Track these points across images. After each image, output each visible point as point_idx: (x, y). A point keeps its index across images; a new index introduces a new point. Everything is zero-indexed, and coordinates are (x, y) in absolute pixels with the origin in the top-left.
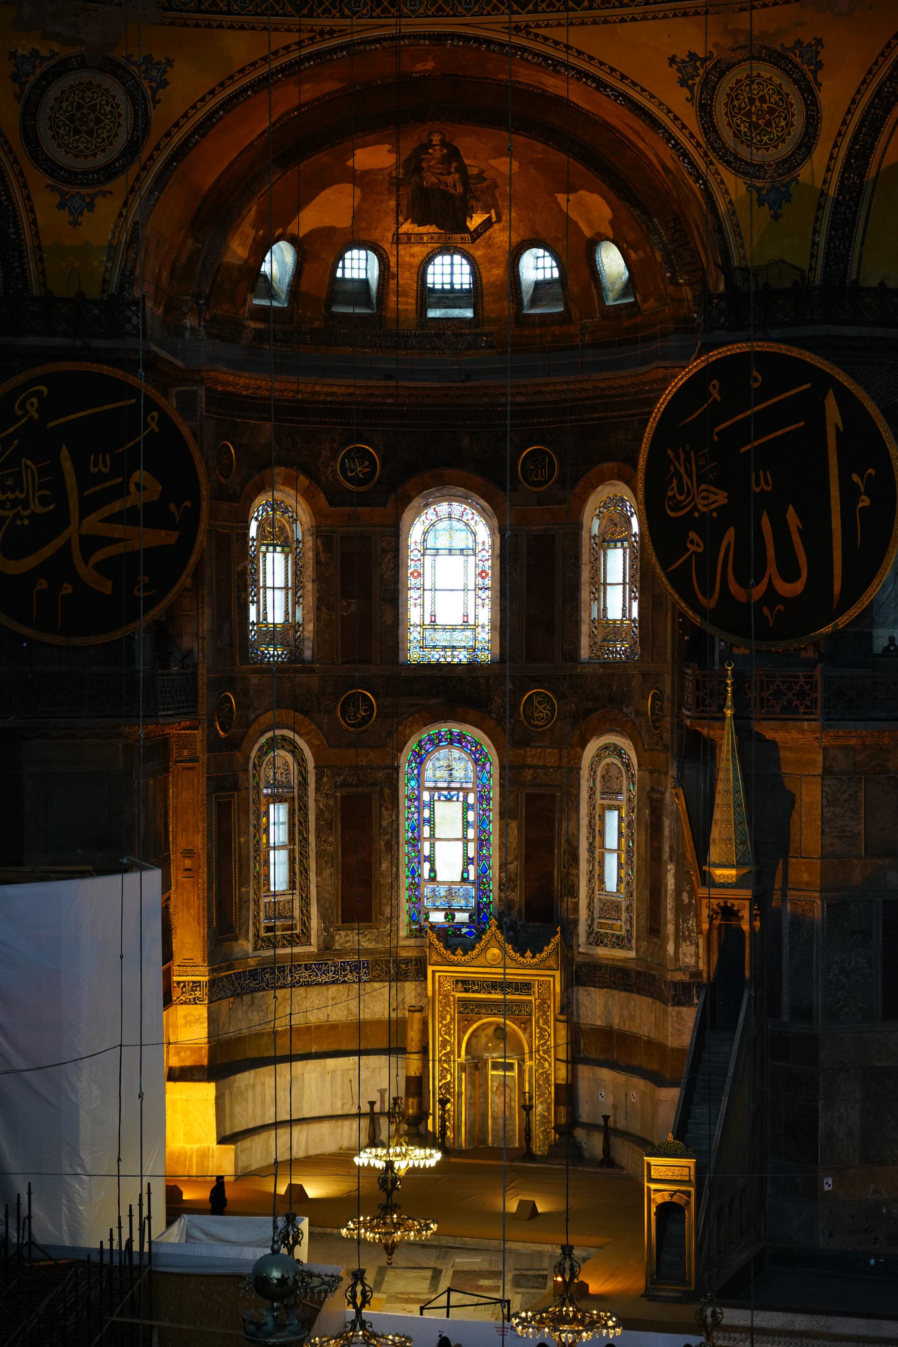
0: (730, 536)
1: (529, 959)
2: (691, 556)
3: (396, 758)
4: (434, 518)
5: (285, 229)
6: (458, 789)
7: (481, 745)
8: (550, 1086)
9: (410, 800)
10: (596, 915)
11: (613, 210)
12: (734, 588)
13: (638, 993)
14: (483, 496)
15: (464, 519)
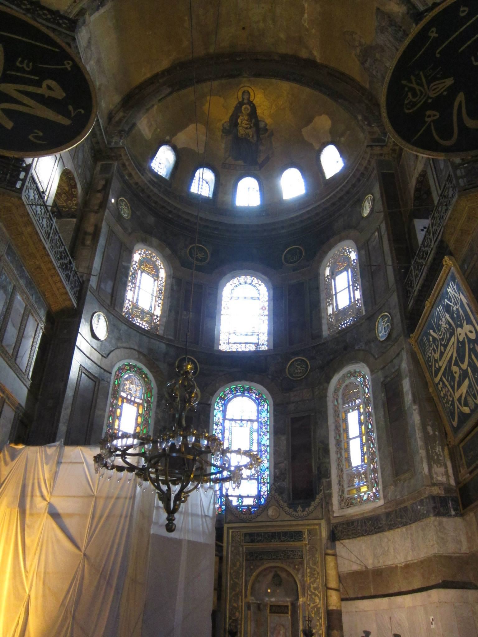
0: (461, 97)
1: (300, 513)
2: (430, 122)
3: (209, 399)
4: (237, 283)
5: (171, 138)
6: (248, 421)
7: (262, 395)
8: (321, 618)
9: (217, 425)
10: (345, 485)
11: (332, 119)
12: (470, 123)
13: (390, 529)
14: (265, 273)
15: (254, 283)
